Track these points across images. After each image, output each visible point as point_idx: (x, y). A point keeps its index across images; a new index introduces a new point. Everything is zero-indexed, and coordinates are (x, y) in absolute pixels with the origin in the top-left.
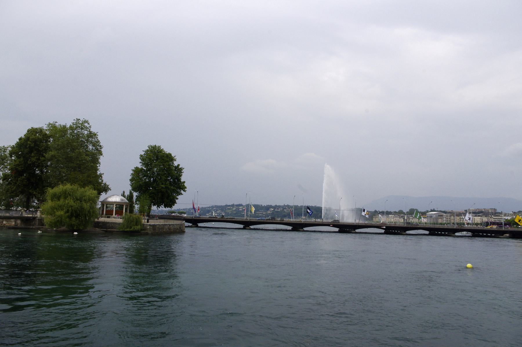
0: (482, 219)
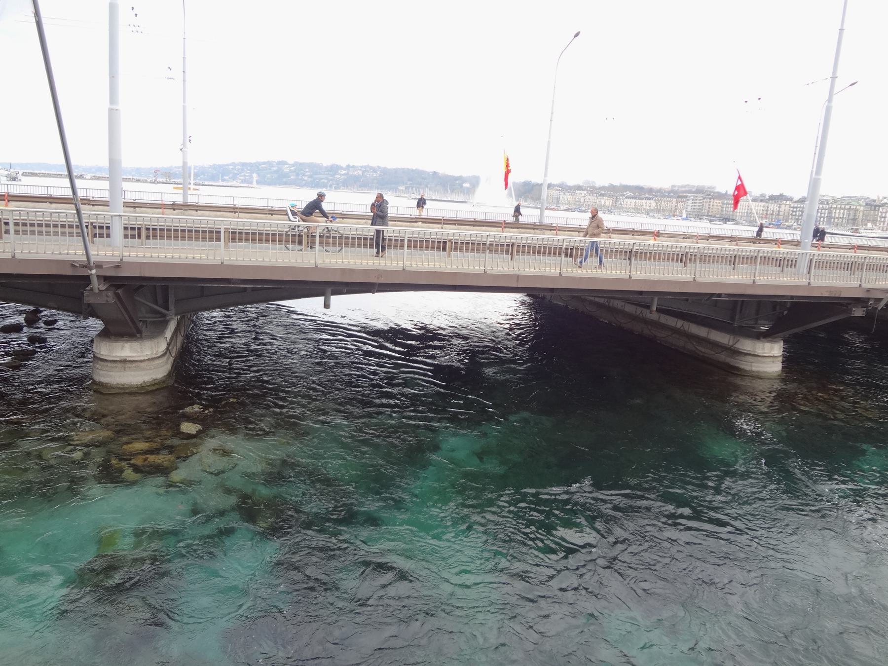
0: (768, 207)
